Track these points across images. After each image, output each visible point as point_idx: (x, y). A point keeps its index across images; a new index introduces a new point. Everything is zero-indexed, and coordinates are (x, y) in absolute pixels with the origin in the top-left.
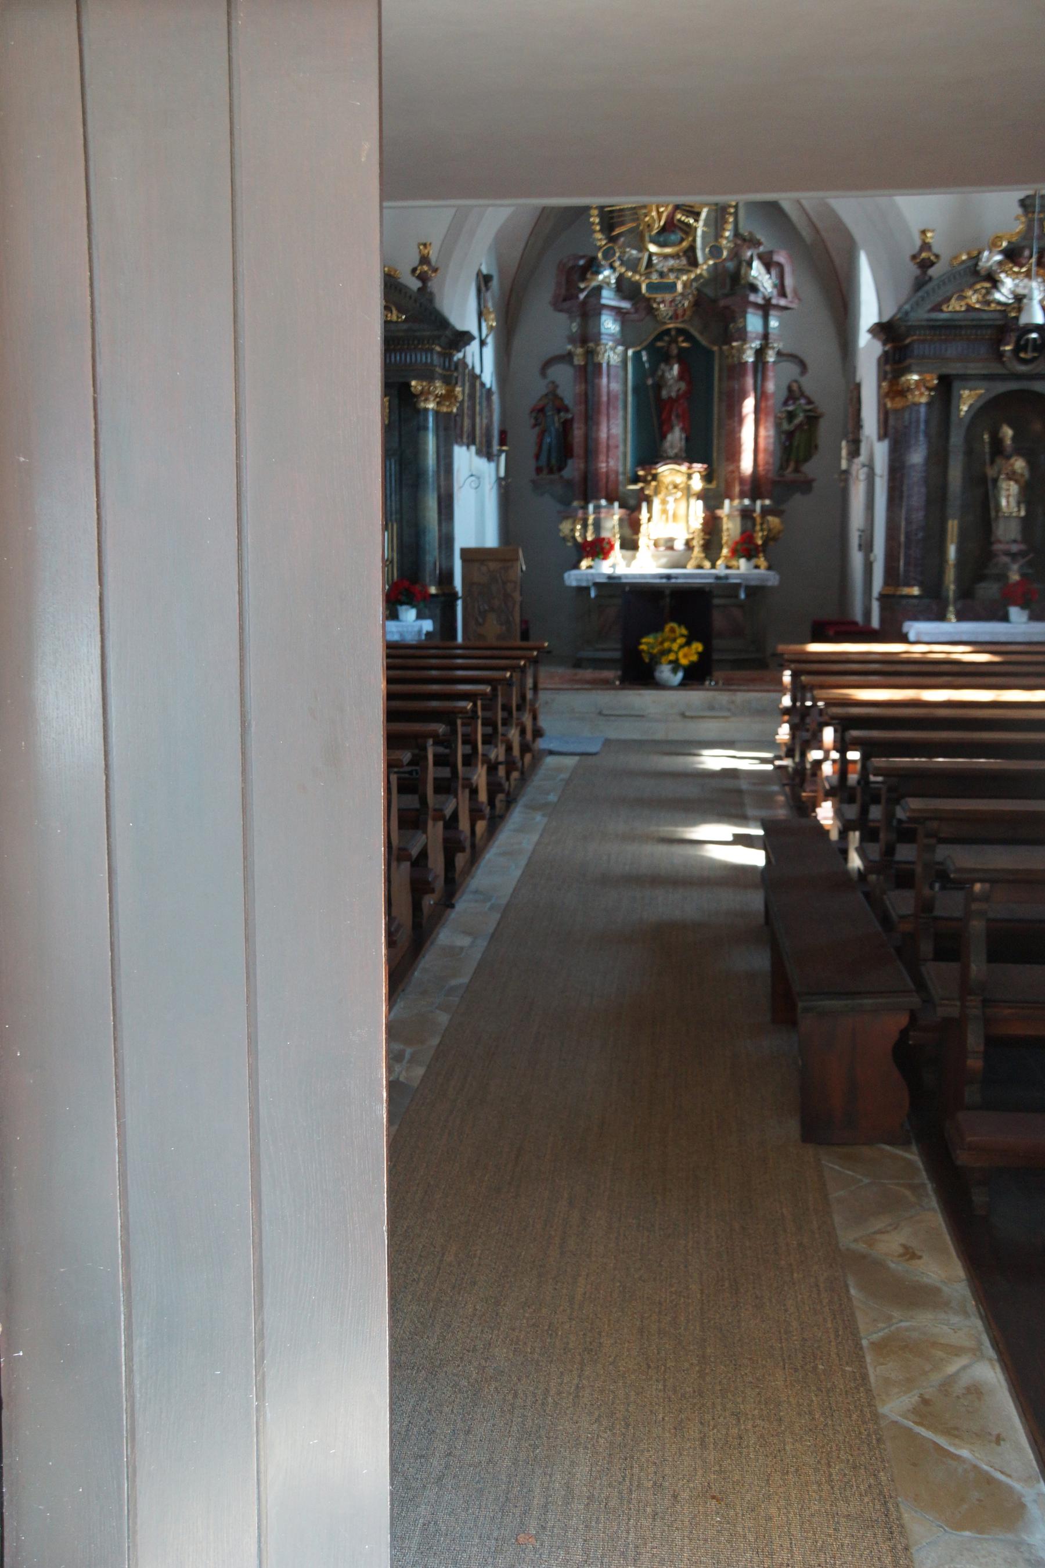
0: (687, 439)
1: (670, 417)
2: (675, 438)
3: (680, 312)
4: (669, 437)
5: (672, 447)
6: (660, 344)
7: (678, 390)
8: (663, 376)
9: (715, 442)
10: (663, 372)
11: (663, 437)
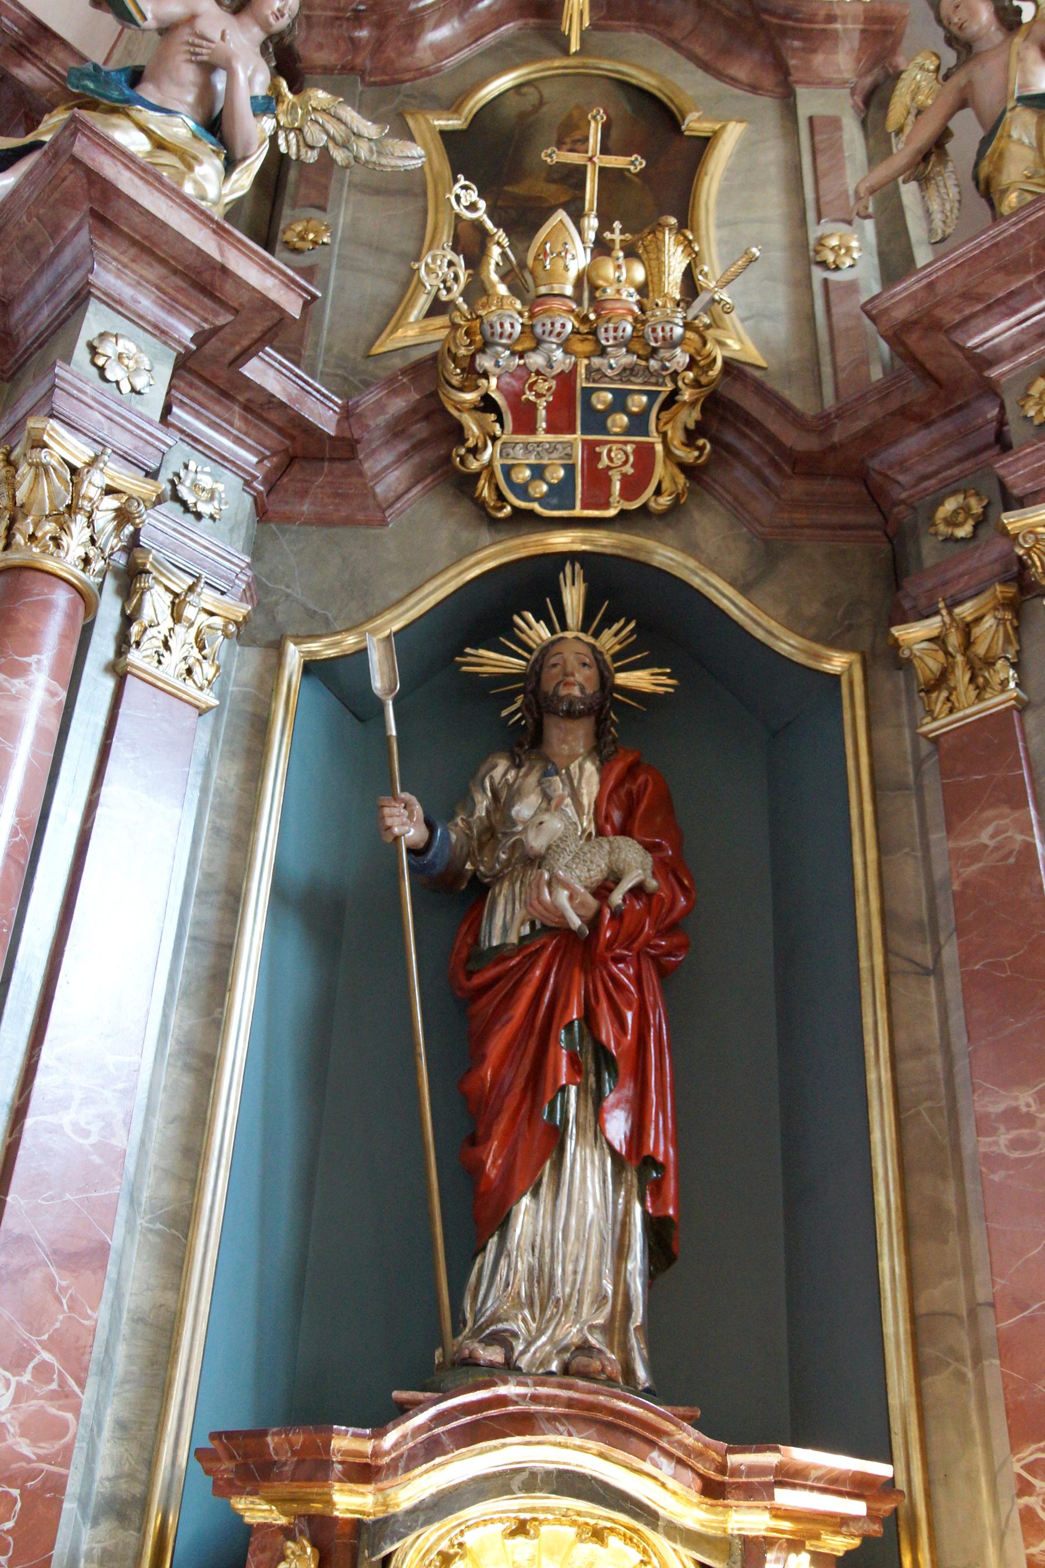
0: (660, 1236)
1: (537, 1079)
2: (575, 1228)
3: (617, 456)
4: (526, 1216)
5: (543, 1294)
6: (491, 661)
7: (602, 891)
8: (498, 827)
9: (890, 1265)
10: (503, 801)
11: (483, 1217)
